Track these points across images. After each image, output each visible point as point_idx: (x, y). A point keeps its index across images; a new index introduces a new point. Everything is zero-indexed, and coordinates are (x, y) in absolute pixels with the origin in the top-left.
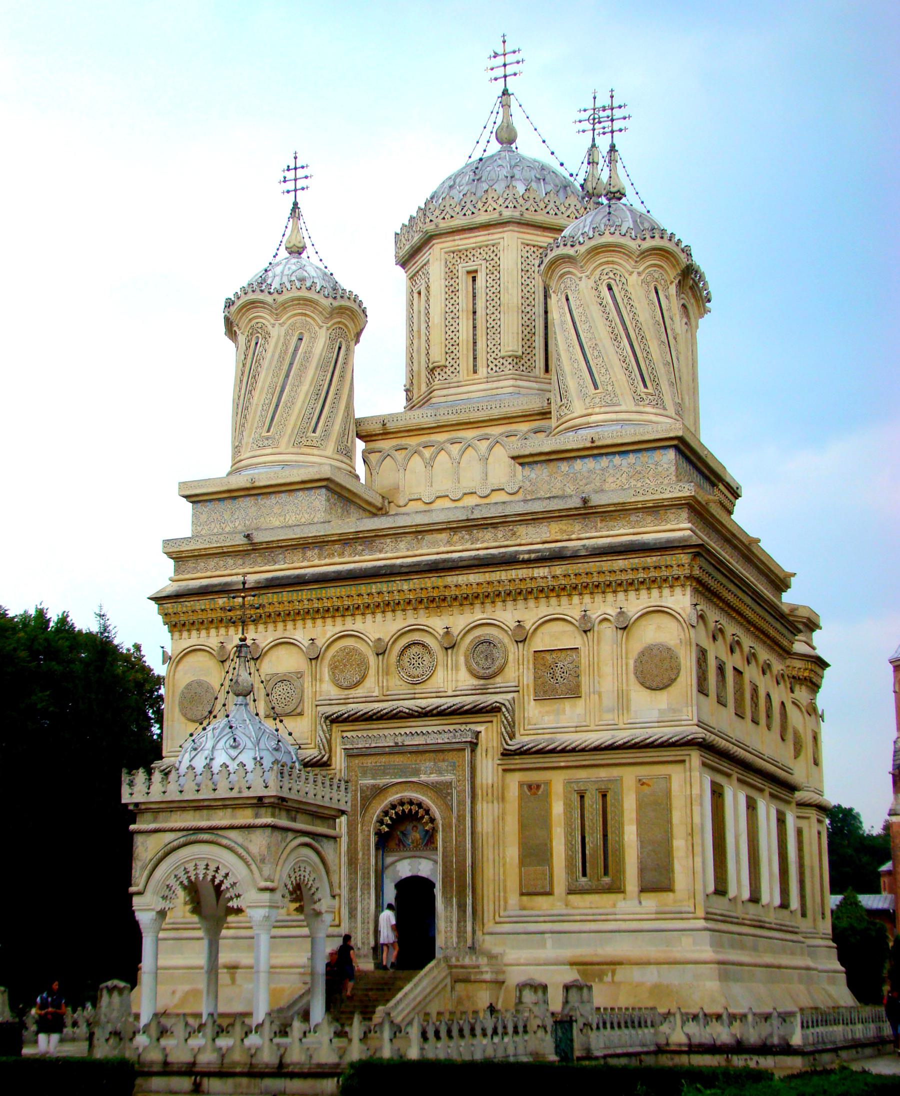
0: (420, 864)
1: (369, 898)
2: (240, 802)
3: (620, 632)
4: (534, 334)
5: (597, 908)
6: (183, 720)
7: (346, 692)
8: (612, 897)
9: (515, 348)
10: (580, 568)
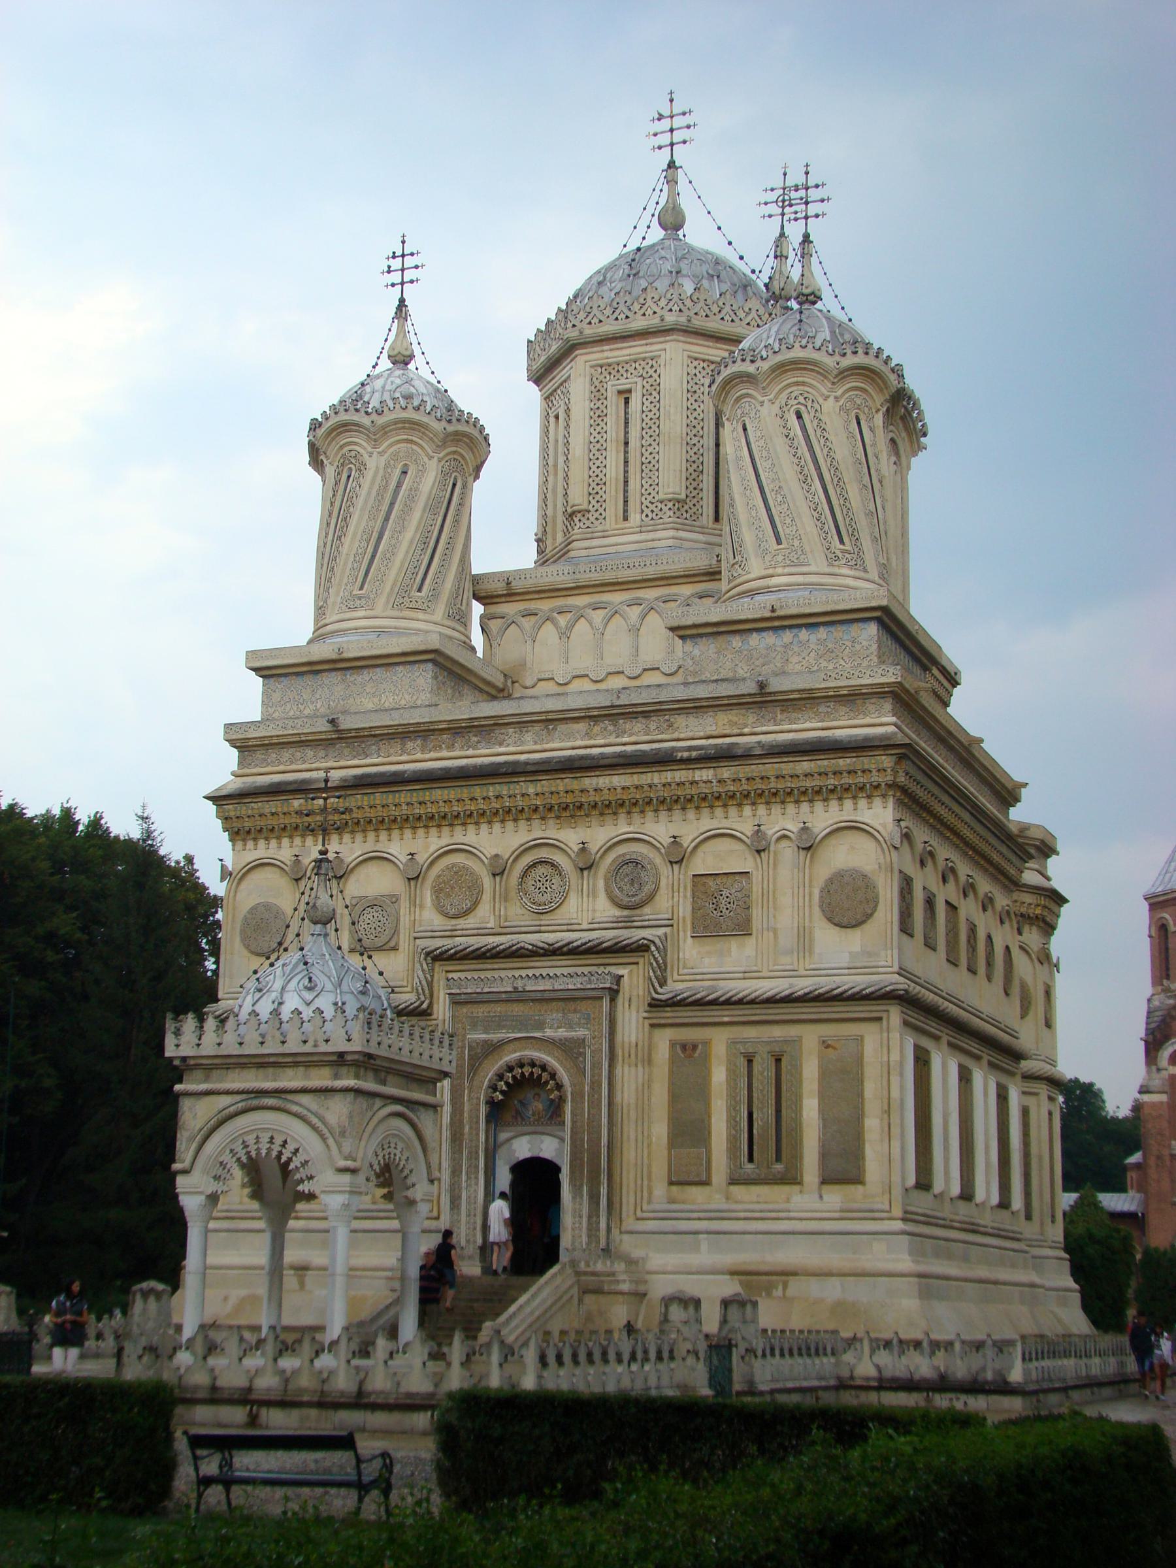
0: (542, 1142)
1: (477, 1184)
2: (315, 1058)
3: (802, 853)
4: (702, 472)
5: (766, 1202)
6: (245, 952)
7: (454, 922)
8: (786, 1189)
9: (677, 490)
10: (753, 771)
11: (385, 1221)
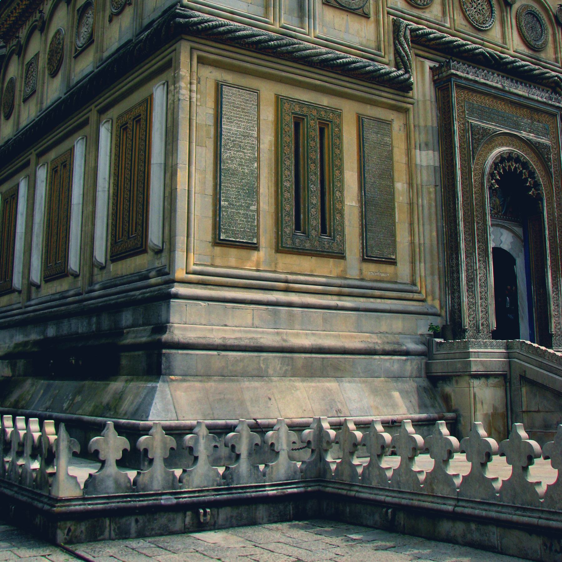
0: (502, 234)
11: (379, 300)
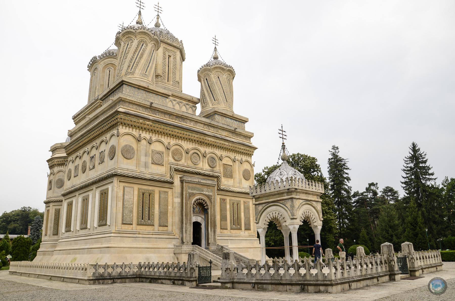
6: (122, 157)
8: (239, 231)
